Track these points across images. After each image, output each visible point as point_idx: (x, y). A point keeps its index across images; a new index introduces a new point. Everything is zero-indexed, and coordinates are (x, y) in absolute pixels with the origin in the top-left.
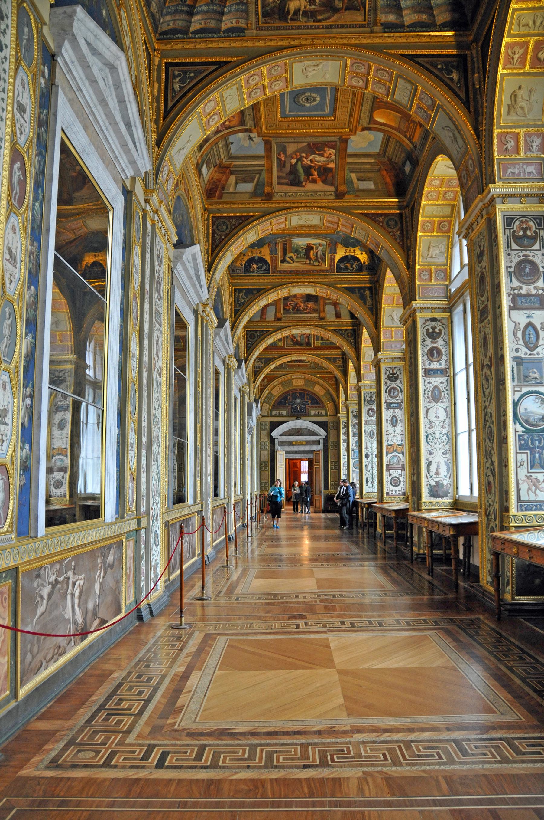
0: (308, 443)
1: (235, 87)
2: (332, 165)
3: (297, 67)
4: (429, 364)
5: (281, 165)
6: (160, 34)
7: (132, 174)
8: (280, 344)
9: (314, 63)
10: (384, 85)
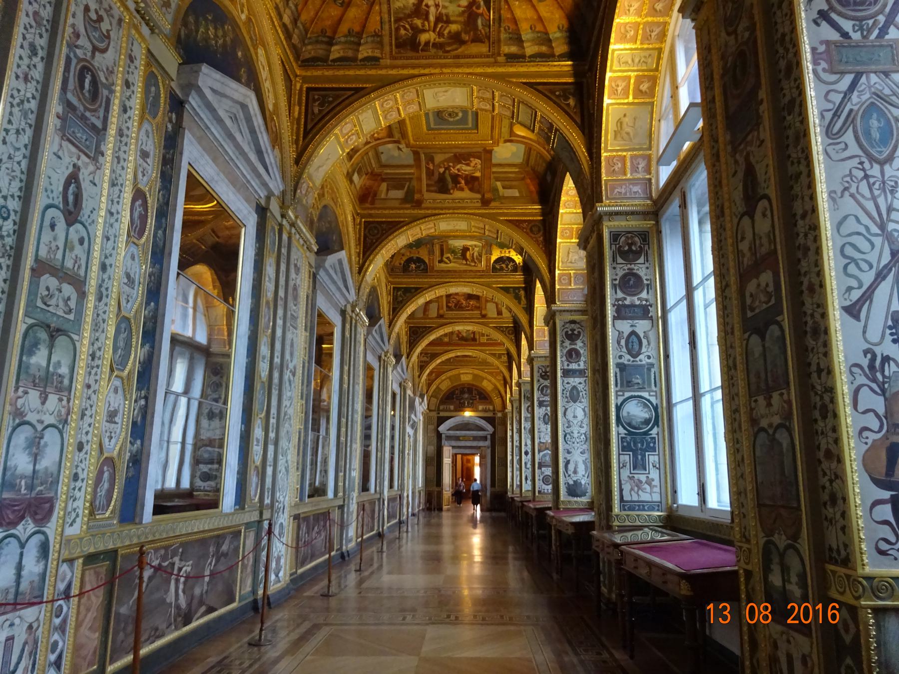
0: (475, 438)
1: (370, 111)
2: (478, 174)
3: (428, 93)
4: (568, 365)
5: (430, 173)
6: (303, 61)
7: (266, 194)
8: (446, 340)
9: (444, 89)
10: (509, 108)
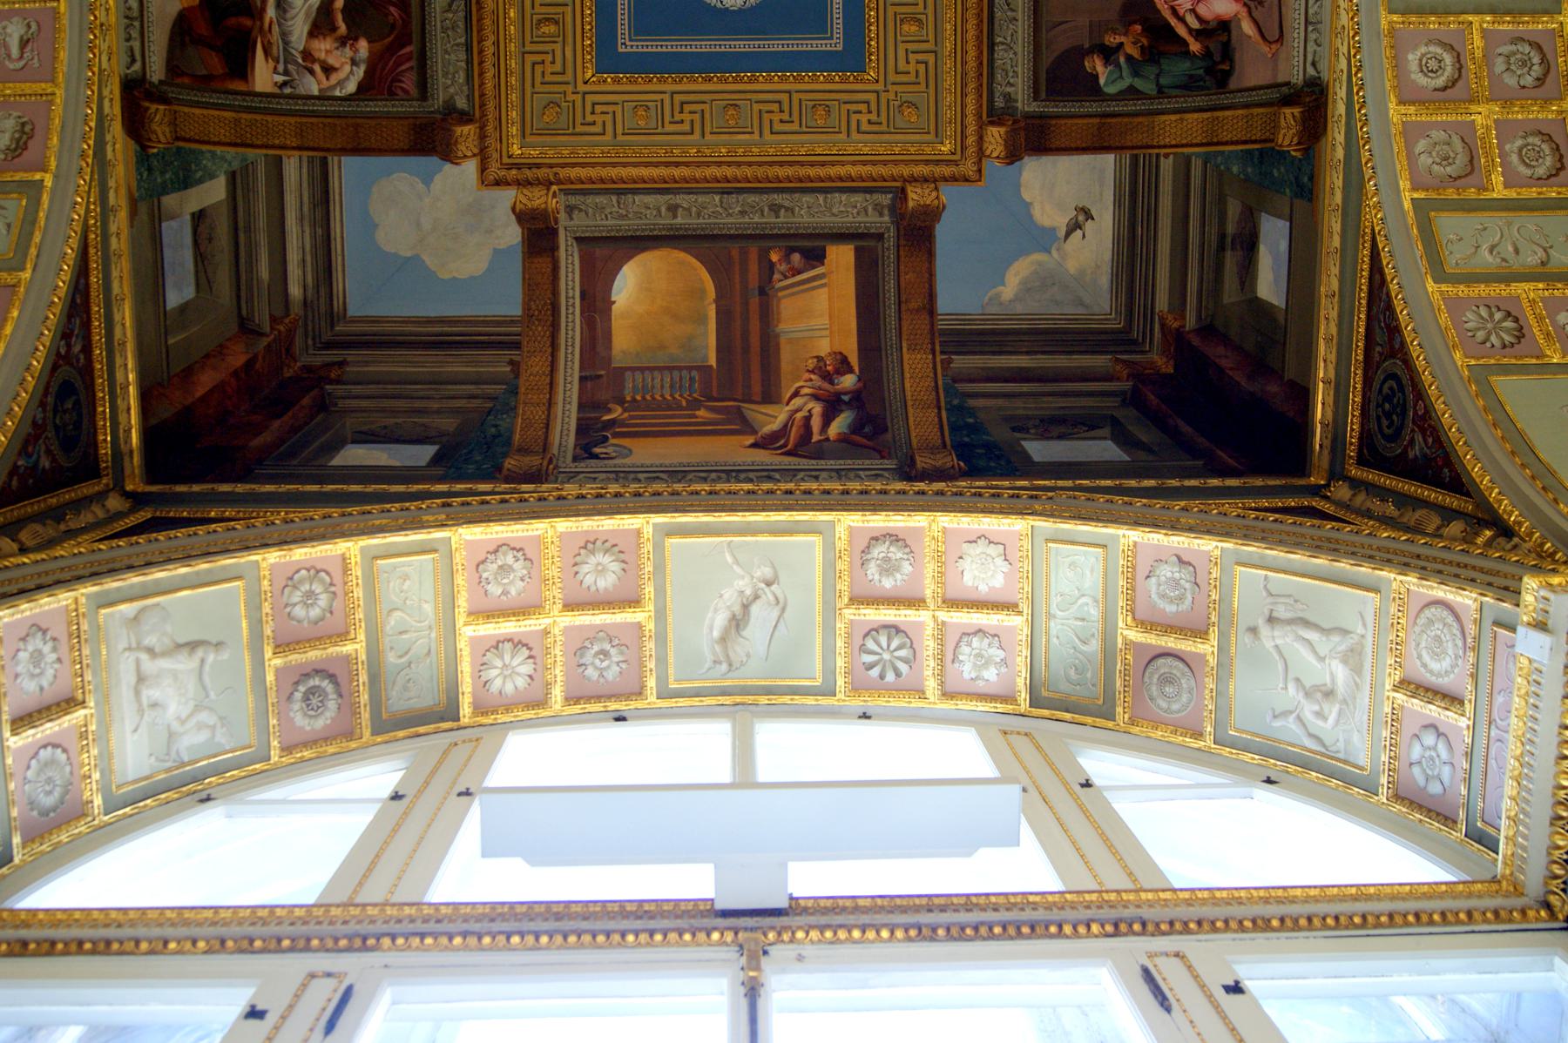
2: (264, 76)
